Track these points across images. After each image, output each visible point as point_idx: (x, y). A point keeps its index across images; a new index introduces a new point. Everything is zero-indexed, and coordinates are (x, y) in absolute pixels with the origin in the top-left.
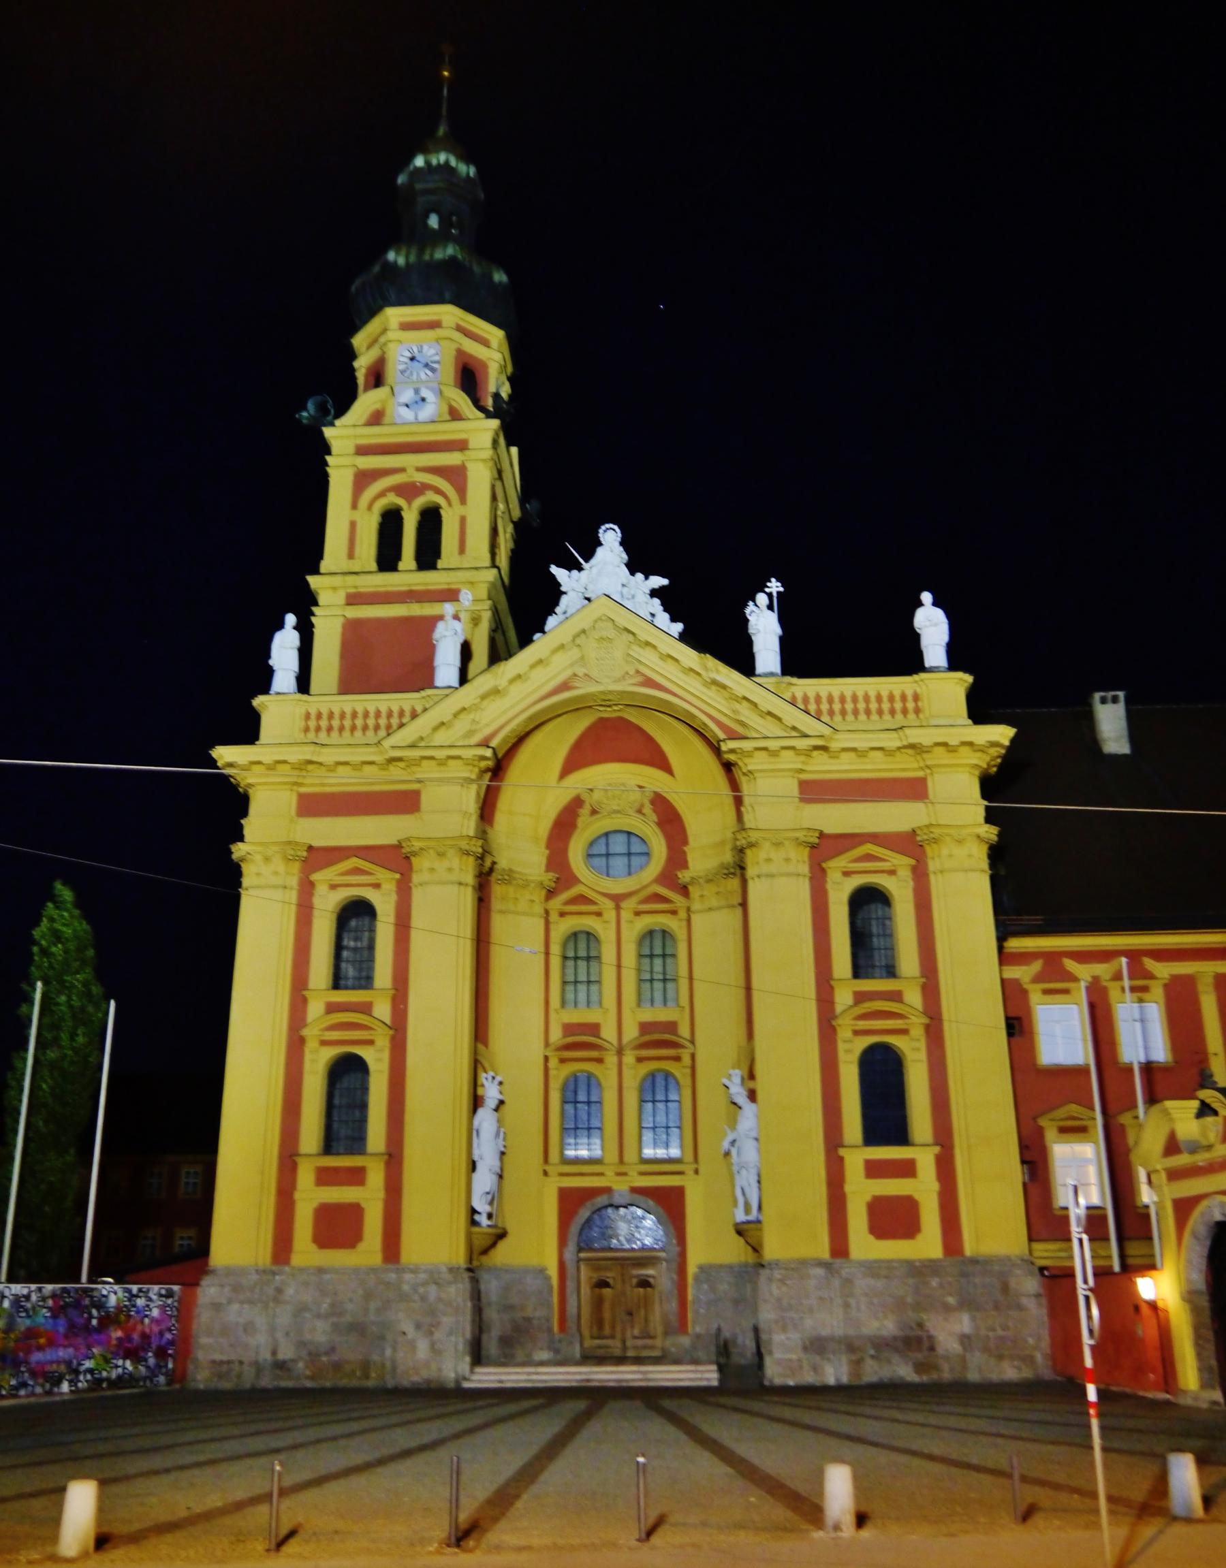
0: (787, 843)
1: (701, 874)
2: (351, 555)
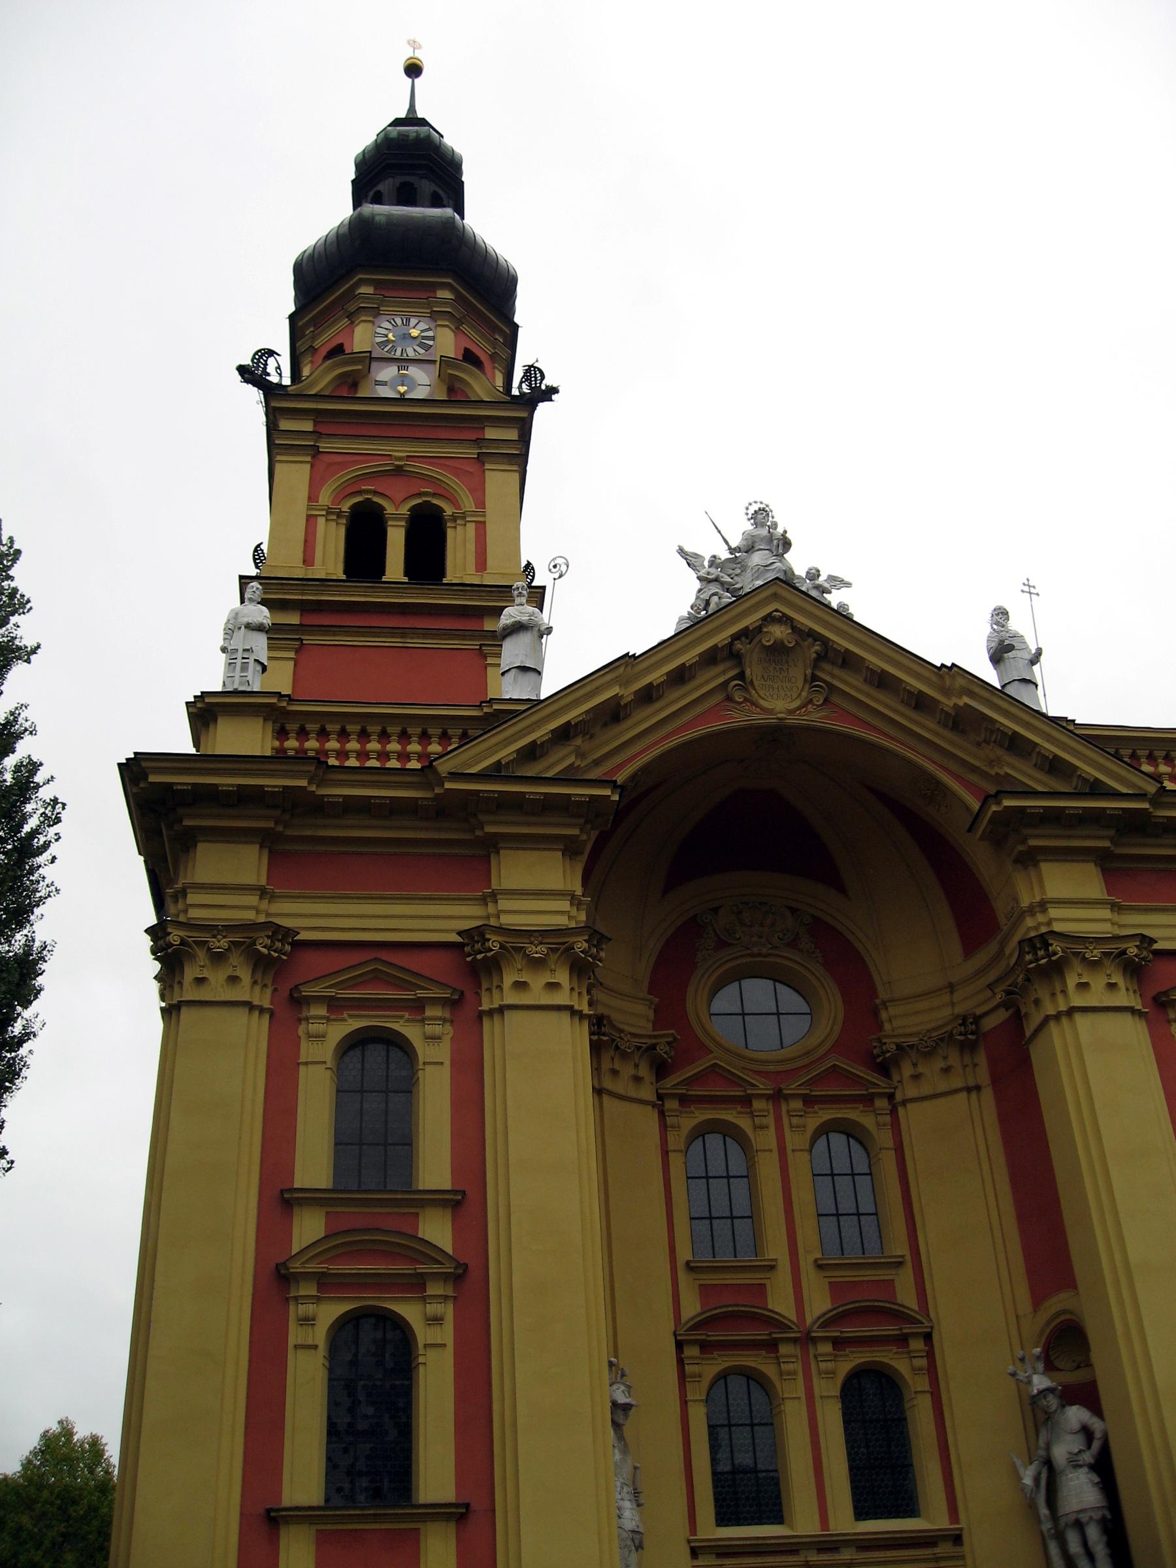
0: (1107, 962)
1: (914, 1040)
2: (308, 560)
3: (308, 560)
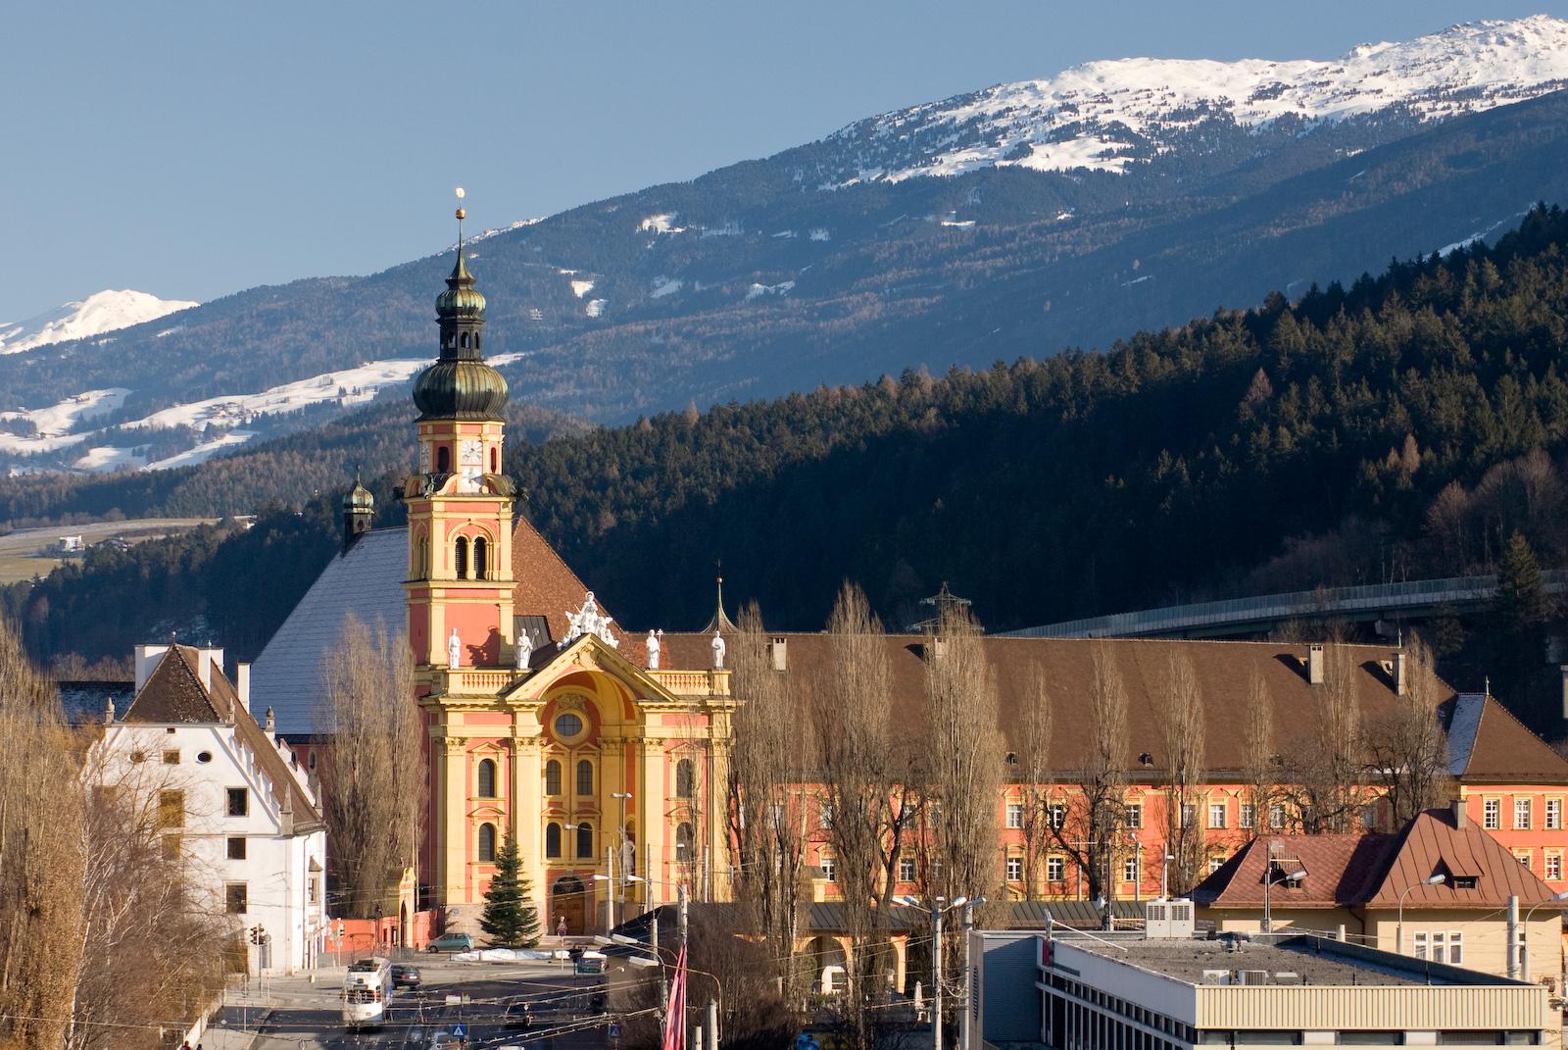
3: (446, 568)
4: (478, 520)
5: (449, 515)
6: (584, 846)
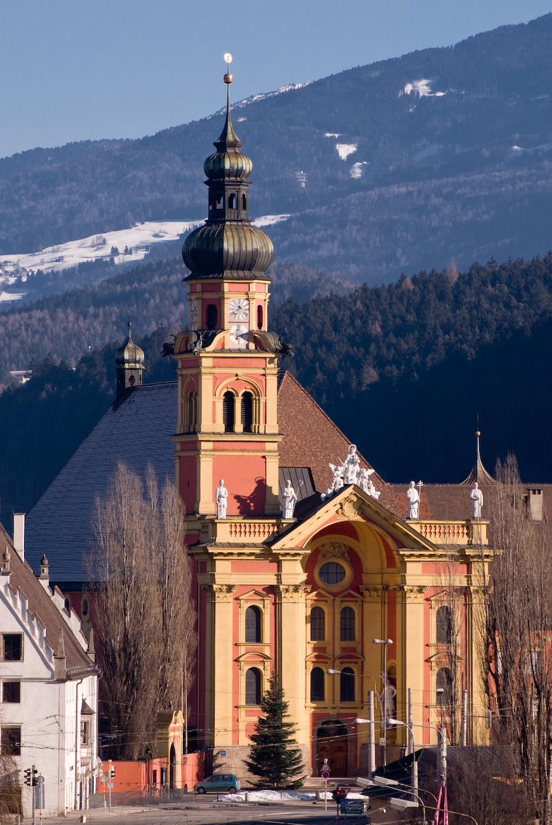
3: (214, 421)
4: (244, 375)
5: (217, 371)
6: (348, 688)
